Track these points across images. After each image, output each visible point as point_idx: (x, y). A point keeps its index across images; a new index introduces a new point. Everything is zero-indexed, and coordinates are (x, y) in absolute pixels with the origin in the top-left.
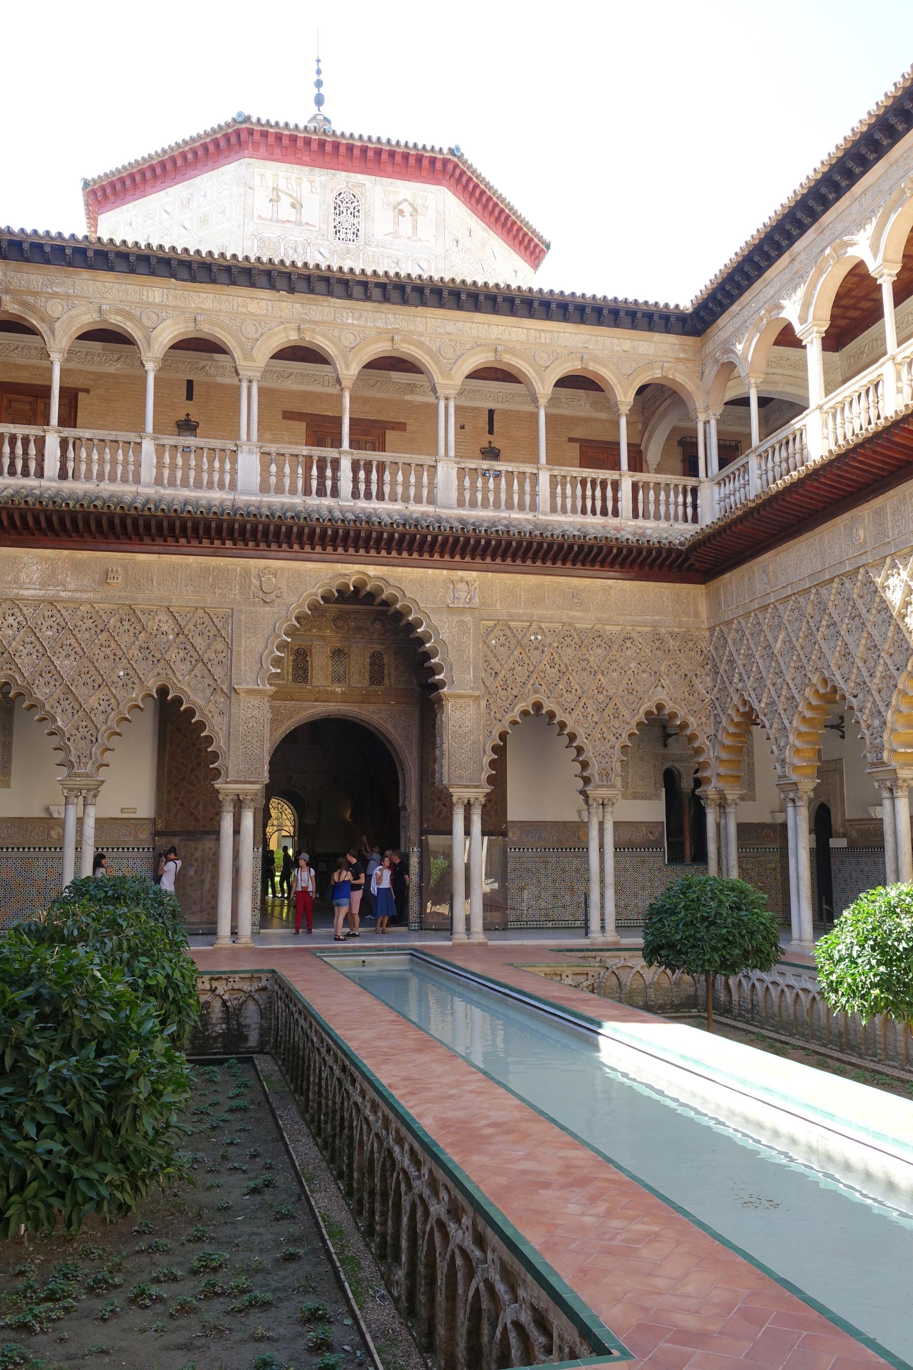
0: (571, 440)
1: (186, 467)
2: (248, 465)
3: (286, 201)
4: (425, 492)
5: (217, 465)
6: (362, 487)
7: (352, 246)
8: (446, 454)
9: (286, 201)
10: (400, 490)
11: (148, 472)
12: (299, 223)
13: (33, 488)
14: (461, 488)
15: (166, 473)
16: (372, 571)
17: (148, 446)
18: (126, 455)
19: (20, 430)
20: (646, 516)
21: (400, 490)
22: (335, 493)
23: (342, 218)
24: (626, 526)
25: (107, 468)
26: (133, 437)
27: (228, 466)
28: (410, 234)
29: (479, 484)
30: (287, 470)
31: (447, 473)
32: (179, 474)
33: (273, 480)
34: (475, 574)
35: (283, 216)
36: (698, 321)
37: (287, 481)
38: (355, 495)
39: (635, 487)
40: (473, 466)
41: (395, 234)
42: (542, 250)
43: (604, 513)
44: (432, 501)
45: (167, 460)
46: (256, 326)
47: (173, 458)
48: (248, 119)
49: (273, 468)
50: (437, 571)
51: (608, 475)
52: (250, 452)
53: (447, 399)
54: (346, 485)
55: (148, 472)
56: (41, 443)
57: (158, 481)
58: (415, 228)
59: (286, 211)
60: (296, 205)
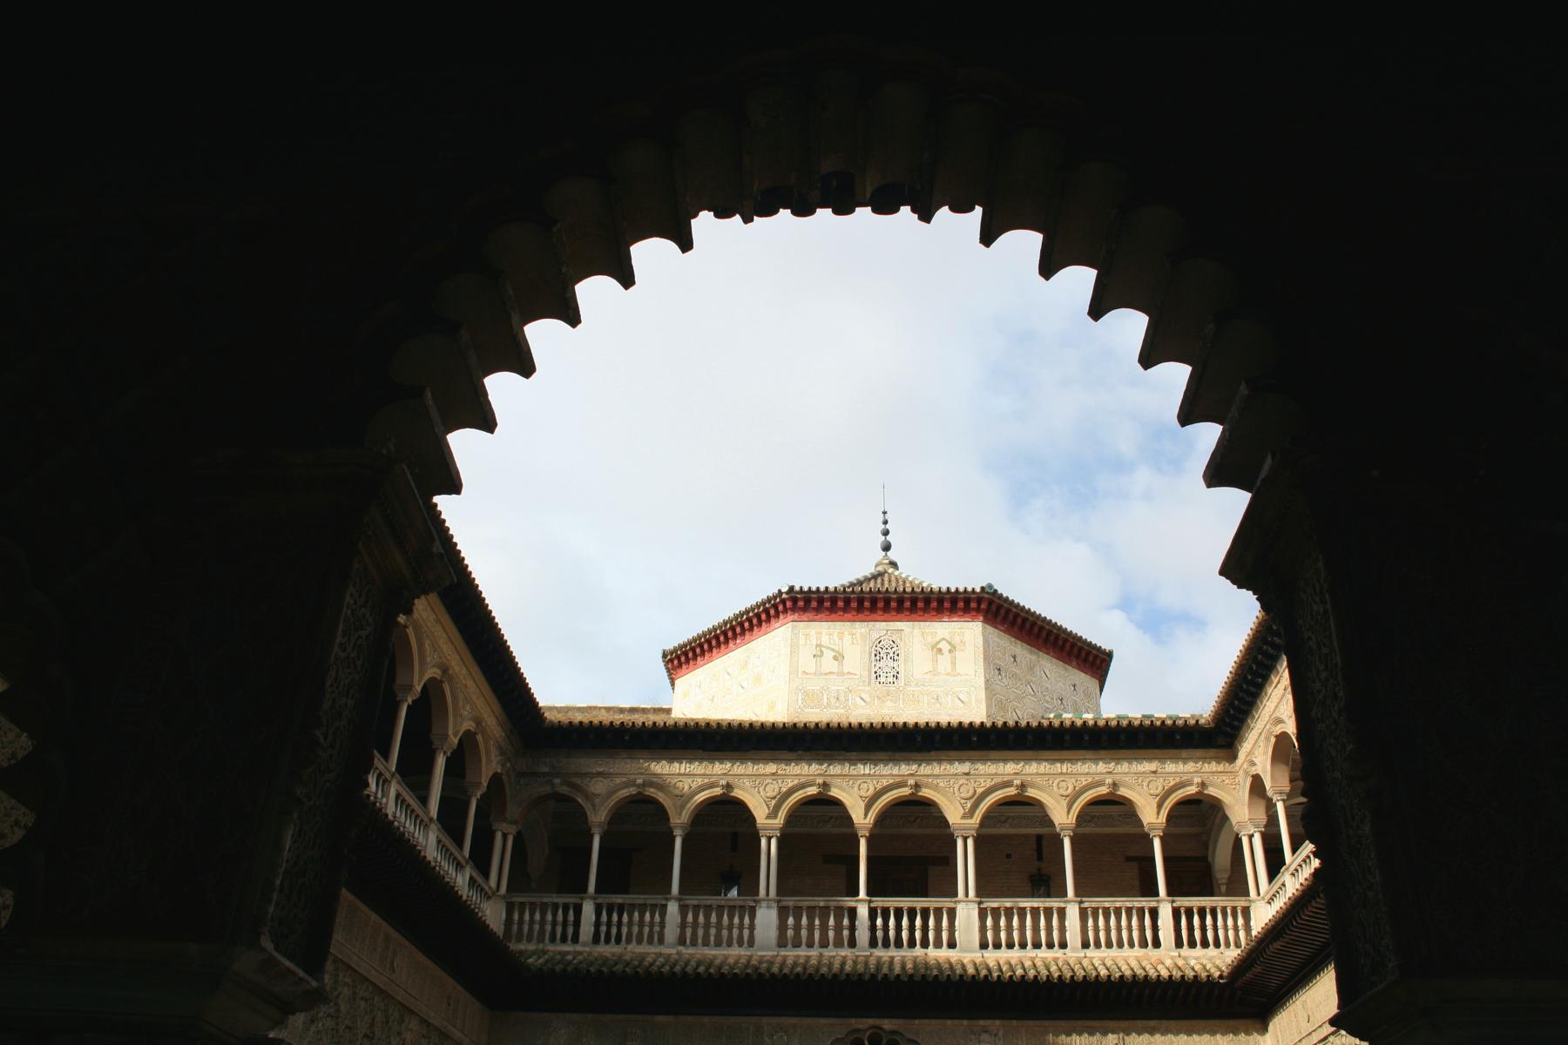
0: (1129, 859)
1: (707, 926)
2: (767, 918)
3: (828, 655)
4: (945, 935)
5: (736, 920)
6: (880, 934)
7: (892, 688)
8: (967, 895)
9: (828, 655)
10: (918, 935)
11: (671, 933)
12: (842, 674)
13: (568, 953)
14: (983, 929)
15: (689, 932)
16: (887, 1024)
17: (673, 908)
18: (652, 917)
19: (561, 900)
20: (1192, 944)
21: (918, 935)
22: (852, 943)
23: (882, 664)
24: (1166, 959)
25: (636, 929)
26: (657, 899)
27: (747, 920)
28: (949, 669)
29: (1003, 922)
30: (804, 921)
31: (967, 915)
32: (700, 932)
33: (790, 933)
34: (997, 1022)
35: (825, 669)
36: (1219, 734)
37: (804, 933)
38: (873, 943)
39: (1176, 913)
40: (995, 905)
41: (934, 672)
42: (1103, 660)
43: (1144, 944)
44: (952, 945)
45: (690, 918)
46: (765, 790)
47: (696, 918)
48: (792, 588)
49: (791, 921)
50: (957, 1022)
51: (1146, 903)
52: (769, 907)
53: (965, 839)
54: (863, 935)
55: (671, 933)
56: (578, 910)
57: (682, 941)
58: (954, 663)
59: (828, 663)
60: (838, 657)
